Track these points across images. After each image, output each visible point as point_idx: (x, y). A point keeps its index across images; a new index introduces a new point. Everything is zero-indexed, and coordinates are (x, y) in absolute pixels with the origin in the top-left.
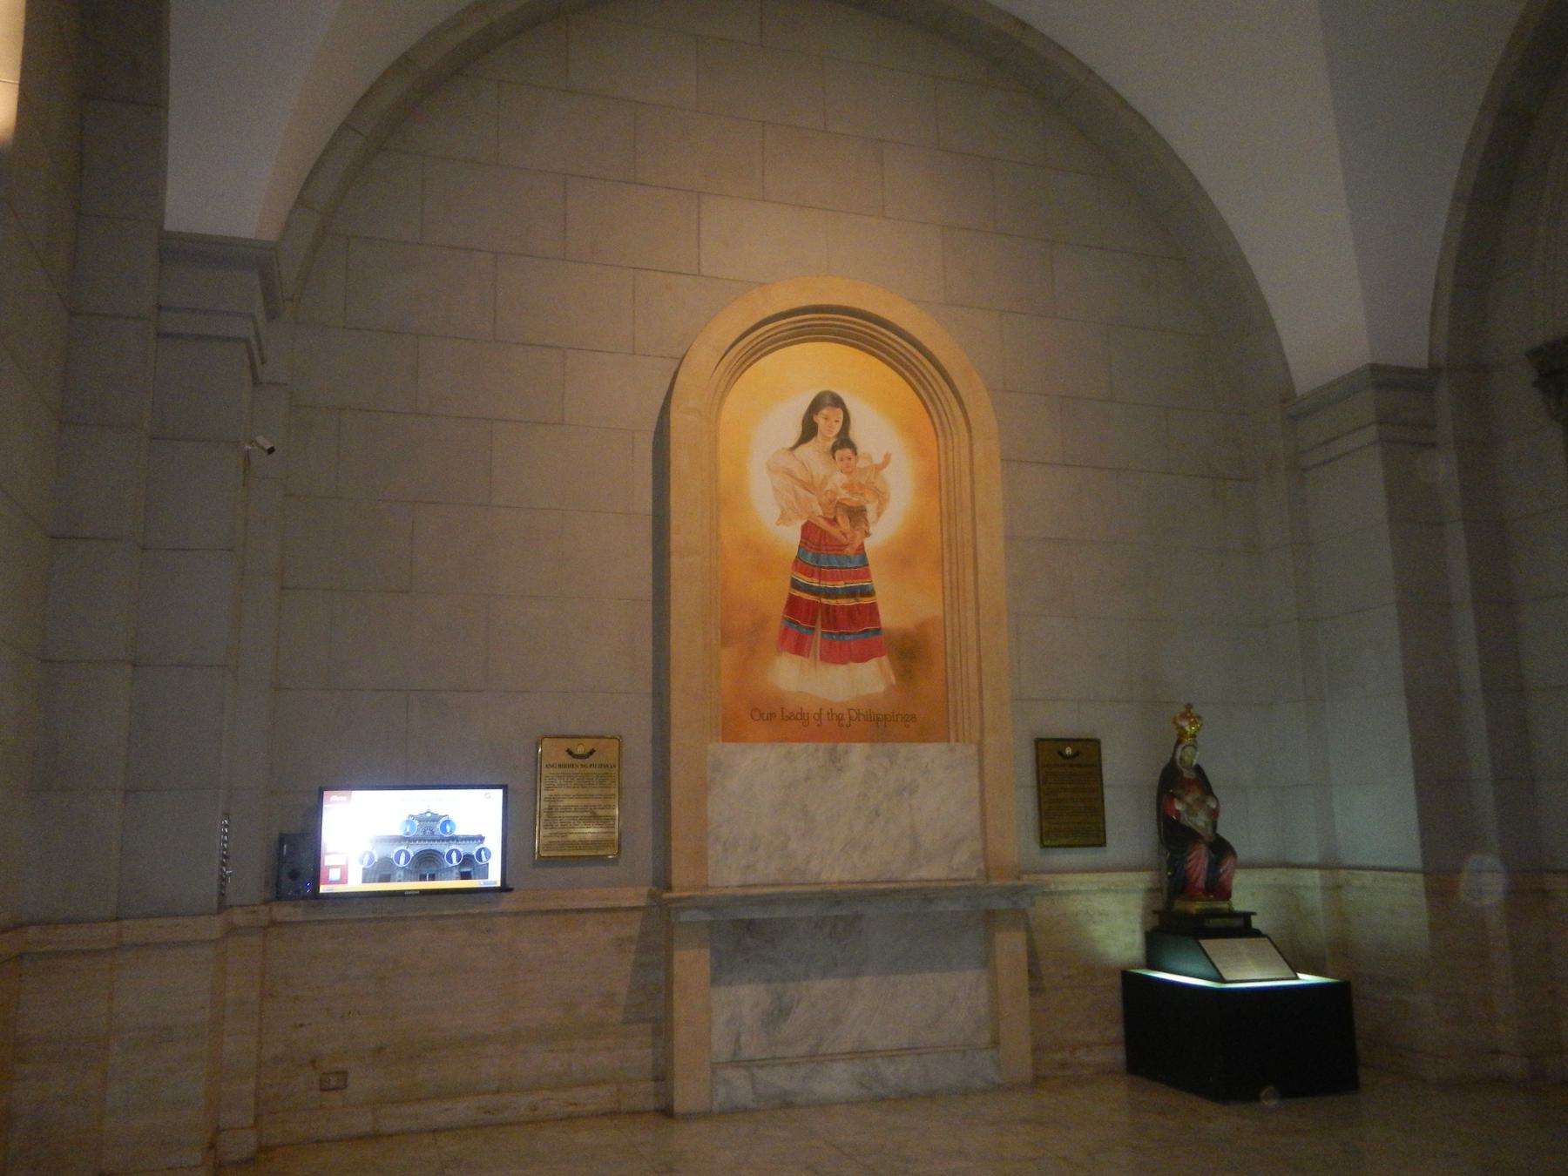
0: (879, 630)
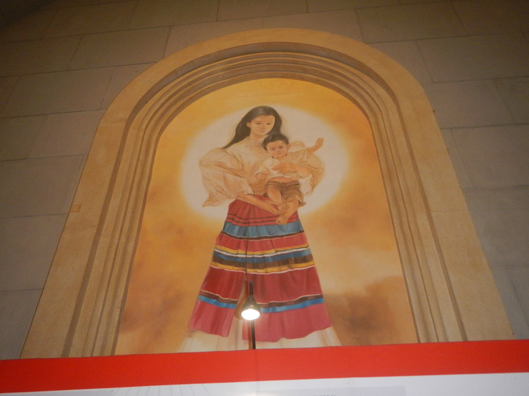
0: (321, 297)
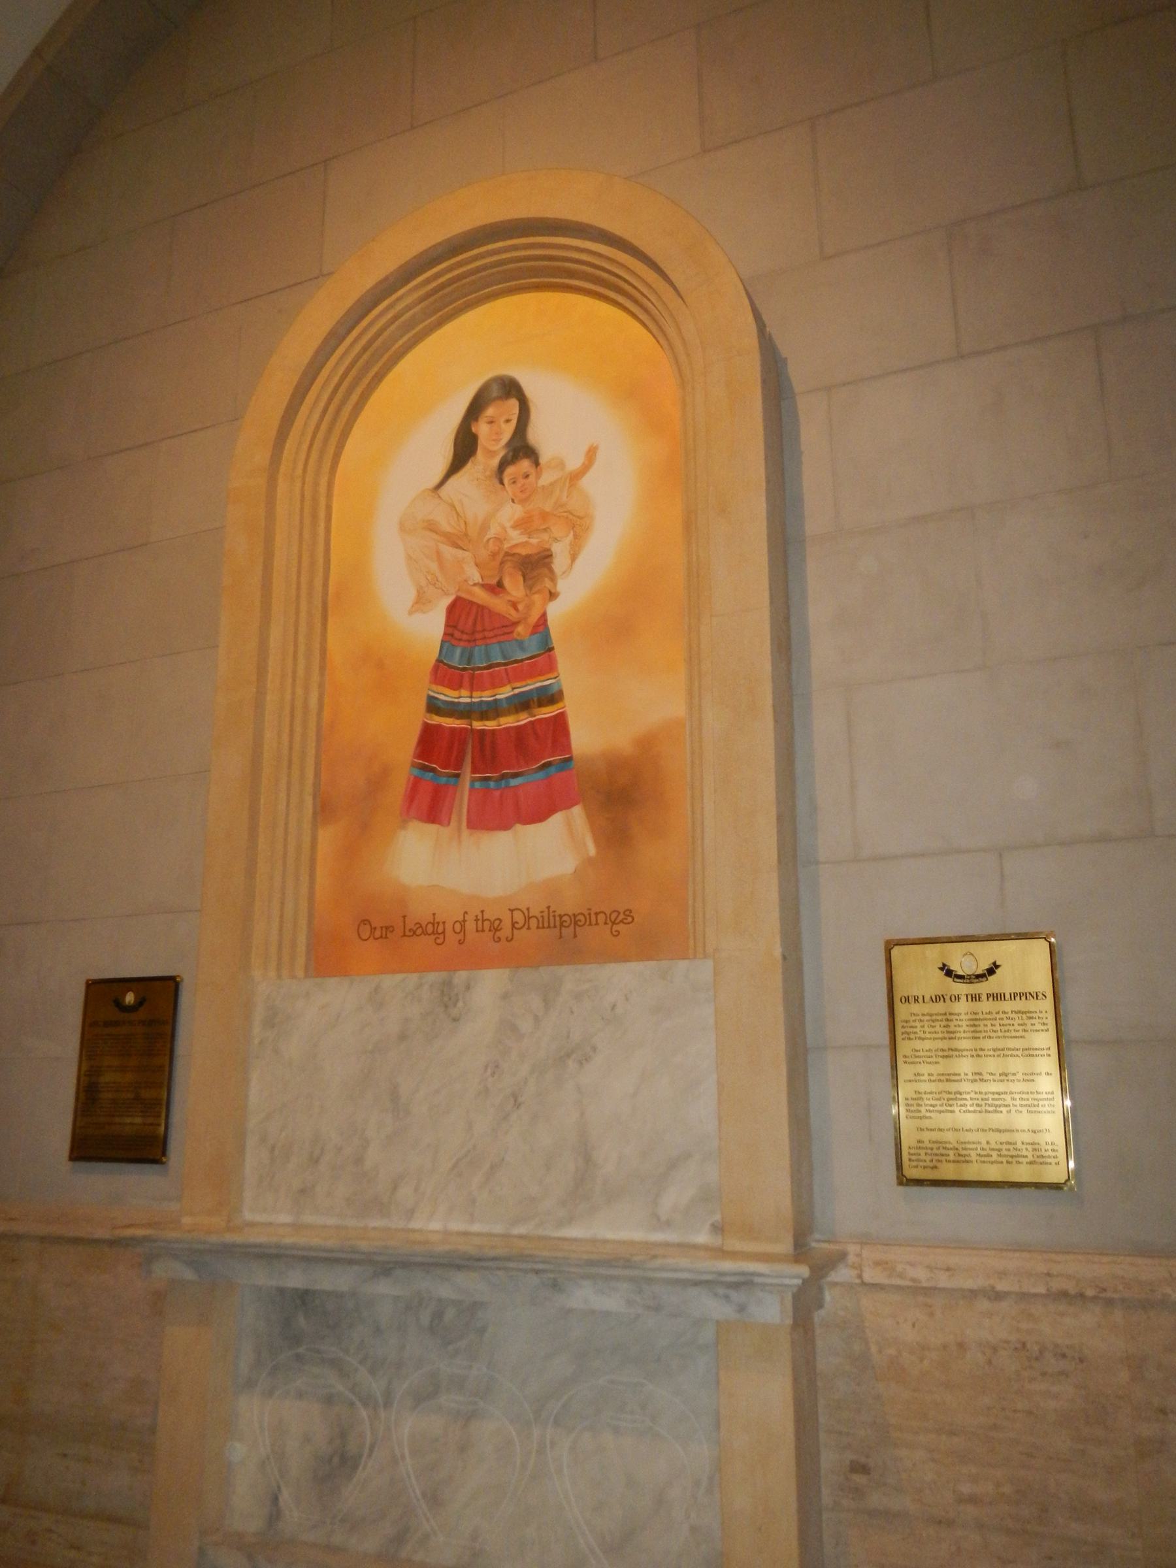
0: (570, 759)
